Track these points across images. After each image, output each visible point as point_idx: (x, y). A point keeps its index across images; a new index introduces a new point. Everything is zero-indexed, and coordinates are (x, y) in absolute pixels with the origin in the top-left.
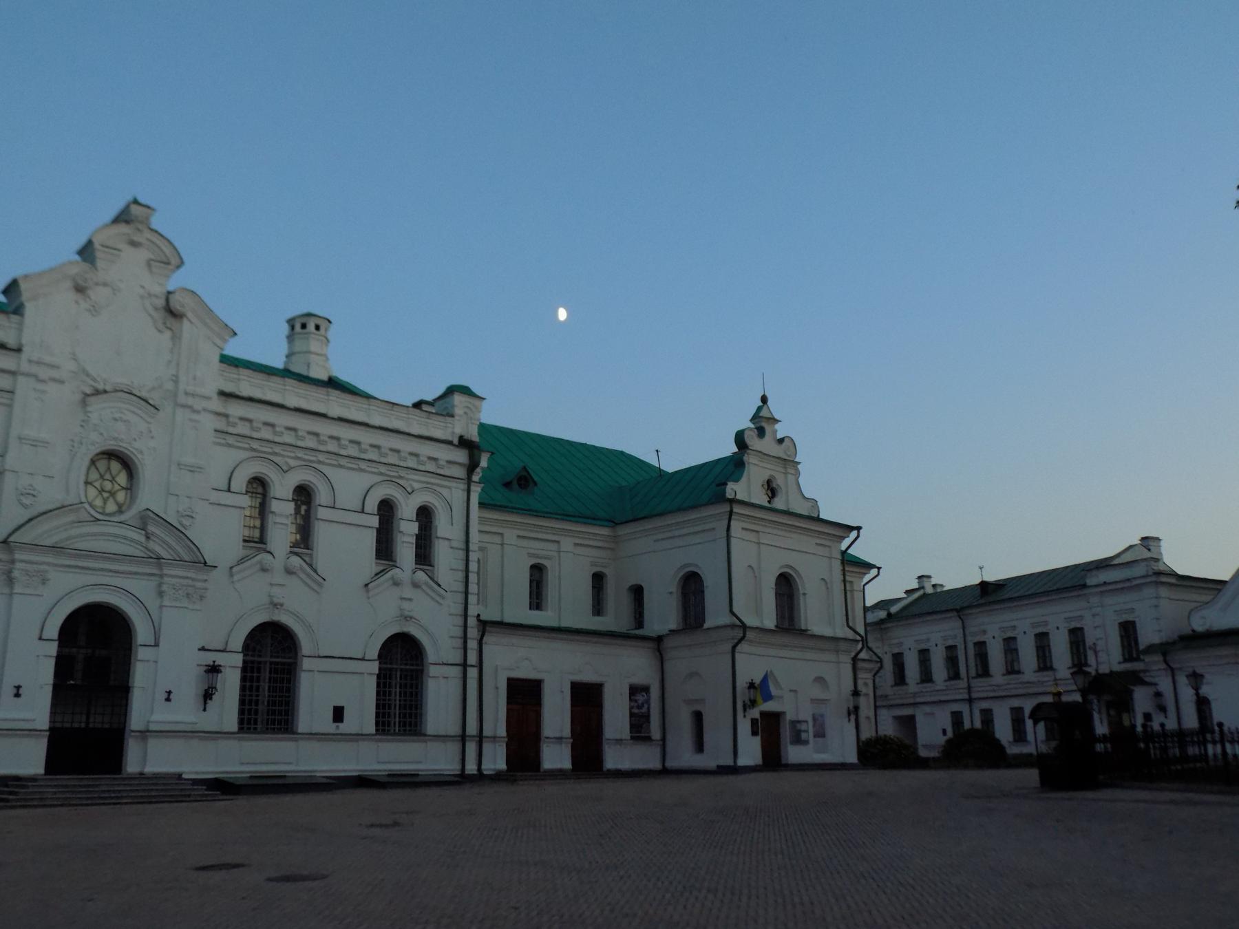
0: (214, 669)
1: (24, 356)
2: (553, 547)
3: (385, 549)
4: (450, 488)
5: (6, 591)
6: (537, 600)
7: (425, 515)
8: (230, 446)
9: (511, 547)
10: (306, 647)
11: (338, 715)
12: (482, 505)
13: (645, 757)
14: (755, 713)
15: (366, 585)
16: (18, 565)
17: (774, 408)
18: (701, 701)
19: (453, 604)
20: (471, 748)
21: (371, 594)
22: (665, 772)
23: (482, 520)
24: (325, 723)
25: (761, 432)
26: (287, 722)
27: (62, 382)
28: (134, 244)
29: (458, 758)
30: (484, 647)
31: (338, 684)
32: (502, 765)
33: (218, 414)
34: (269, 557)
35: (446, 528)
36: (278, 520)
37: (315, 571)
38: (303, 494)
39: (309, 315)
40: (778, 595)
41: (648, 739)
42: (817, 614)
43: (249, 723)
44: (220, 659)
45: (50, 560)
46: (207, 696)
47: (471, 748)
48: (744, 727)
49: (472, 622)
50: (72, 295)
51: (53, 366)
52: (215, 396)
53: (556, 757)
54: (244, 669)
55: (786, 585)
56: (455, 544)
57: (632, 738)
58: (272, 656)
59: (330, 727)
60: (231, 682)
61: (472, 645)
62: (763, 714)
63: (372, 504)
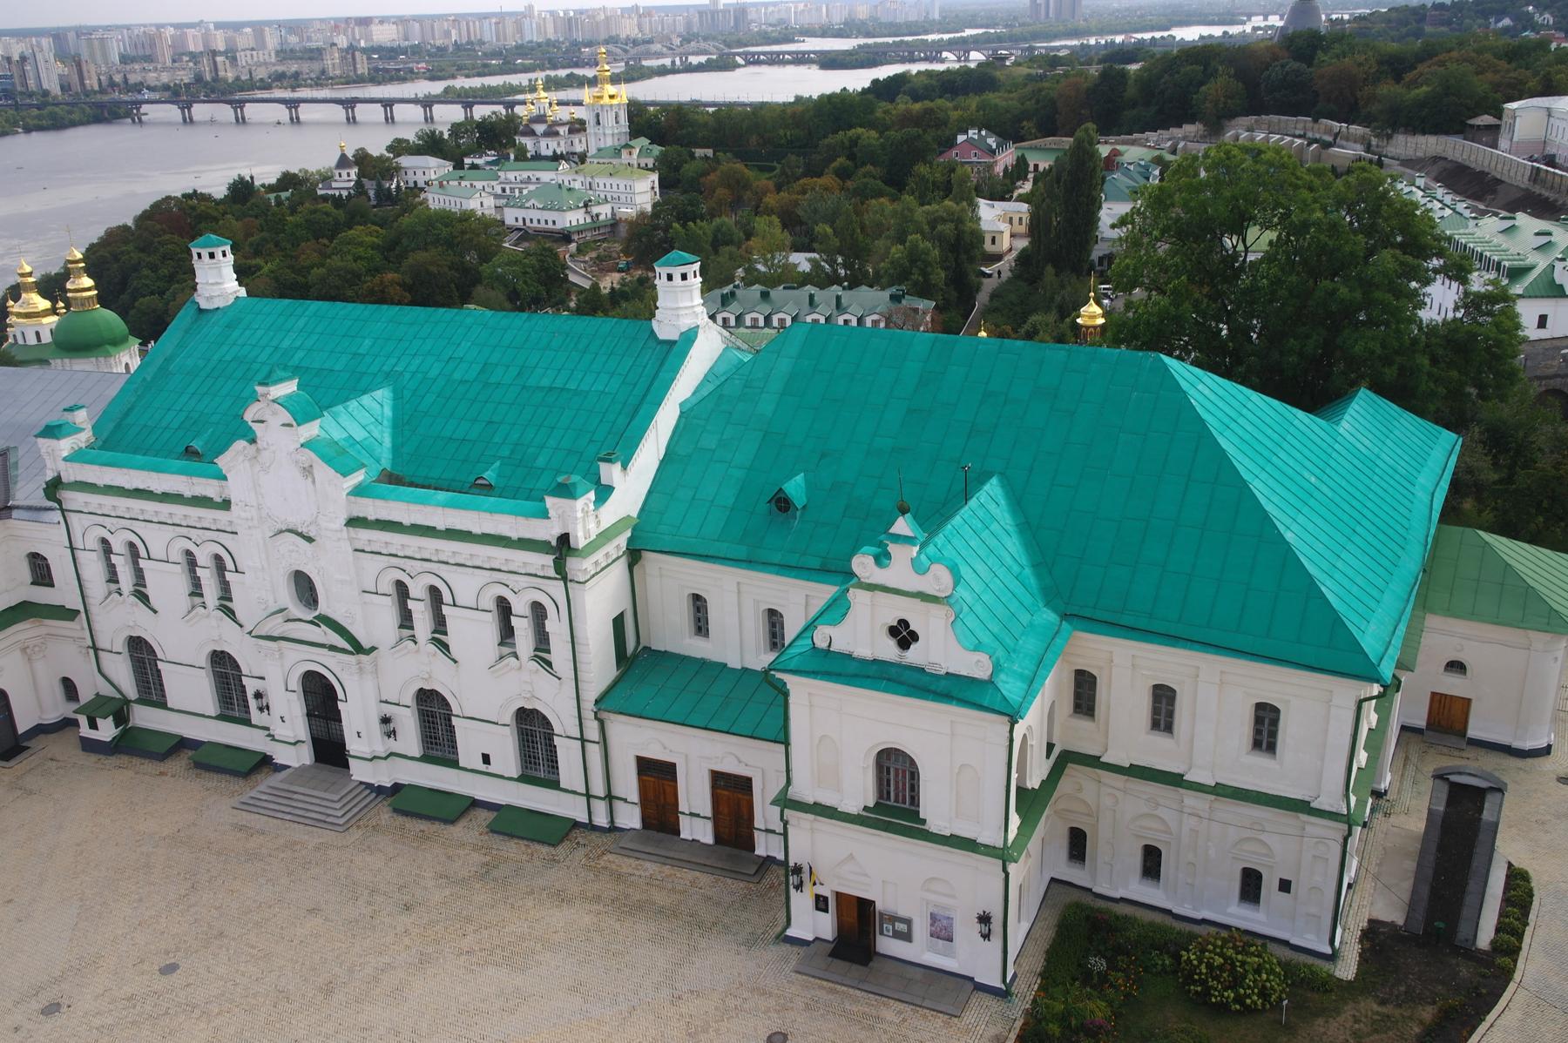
7: (538, 611)
10: (455, 710)
11: (486, 759)
35: (555, 626)
38: (435, 593)
44: (389, 710)
58: (434, 712)
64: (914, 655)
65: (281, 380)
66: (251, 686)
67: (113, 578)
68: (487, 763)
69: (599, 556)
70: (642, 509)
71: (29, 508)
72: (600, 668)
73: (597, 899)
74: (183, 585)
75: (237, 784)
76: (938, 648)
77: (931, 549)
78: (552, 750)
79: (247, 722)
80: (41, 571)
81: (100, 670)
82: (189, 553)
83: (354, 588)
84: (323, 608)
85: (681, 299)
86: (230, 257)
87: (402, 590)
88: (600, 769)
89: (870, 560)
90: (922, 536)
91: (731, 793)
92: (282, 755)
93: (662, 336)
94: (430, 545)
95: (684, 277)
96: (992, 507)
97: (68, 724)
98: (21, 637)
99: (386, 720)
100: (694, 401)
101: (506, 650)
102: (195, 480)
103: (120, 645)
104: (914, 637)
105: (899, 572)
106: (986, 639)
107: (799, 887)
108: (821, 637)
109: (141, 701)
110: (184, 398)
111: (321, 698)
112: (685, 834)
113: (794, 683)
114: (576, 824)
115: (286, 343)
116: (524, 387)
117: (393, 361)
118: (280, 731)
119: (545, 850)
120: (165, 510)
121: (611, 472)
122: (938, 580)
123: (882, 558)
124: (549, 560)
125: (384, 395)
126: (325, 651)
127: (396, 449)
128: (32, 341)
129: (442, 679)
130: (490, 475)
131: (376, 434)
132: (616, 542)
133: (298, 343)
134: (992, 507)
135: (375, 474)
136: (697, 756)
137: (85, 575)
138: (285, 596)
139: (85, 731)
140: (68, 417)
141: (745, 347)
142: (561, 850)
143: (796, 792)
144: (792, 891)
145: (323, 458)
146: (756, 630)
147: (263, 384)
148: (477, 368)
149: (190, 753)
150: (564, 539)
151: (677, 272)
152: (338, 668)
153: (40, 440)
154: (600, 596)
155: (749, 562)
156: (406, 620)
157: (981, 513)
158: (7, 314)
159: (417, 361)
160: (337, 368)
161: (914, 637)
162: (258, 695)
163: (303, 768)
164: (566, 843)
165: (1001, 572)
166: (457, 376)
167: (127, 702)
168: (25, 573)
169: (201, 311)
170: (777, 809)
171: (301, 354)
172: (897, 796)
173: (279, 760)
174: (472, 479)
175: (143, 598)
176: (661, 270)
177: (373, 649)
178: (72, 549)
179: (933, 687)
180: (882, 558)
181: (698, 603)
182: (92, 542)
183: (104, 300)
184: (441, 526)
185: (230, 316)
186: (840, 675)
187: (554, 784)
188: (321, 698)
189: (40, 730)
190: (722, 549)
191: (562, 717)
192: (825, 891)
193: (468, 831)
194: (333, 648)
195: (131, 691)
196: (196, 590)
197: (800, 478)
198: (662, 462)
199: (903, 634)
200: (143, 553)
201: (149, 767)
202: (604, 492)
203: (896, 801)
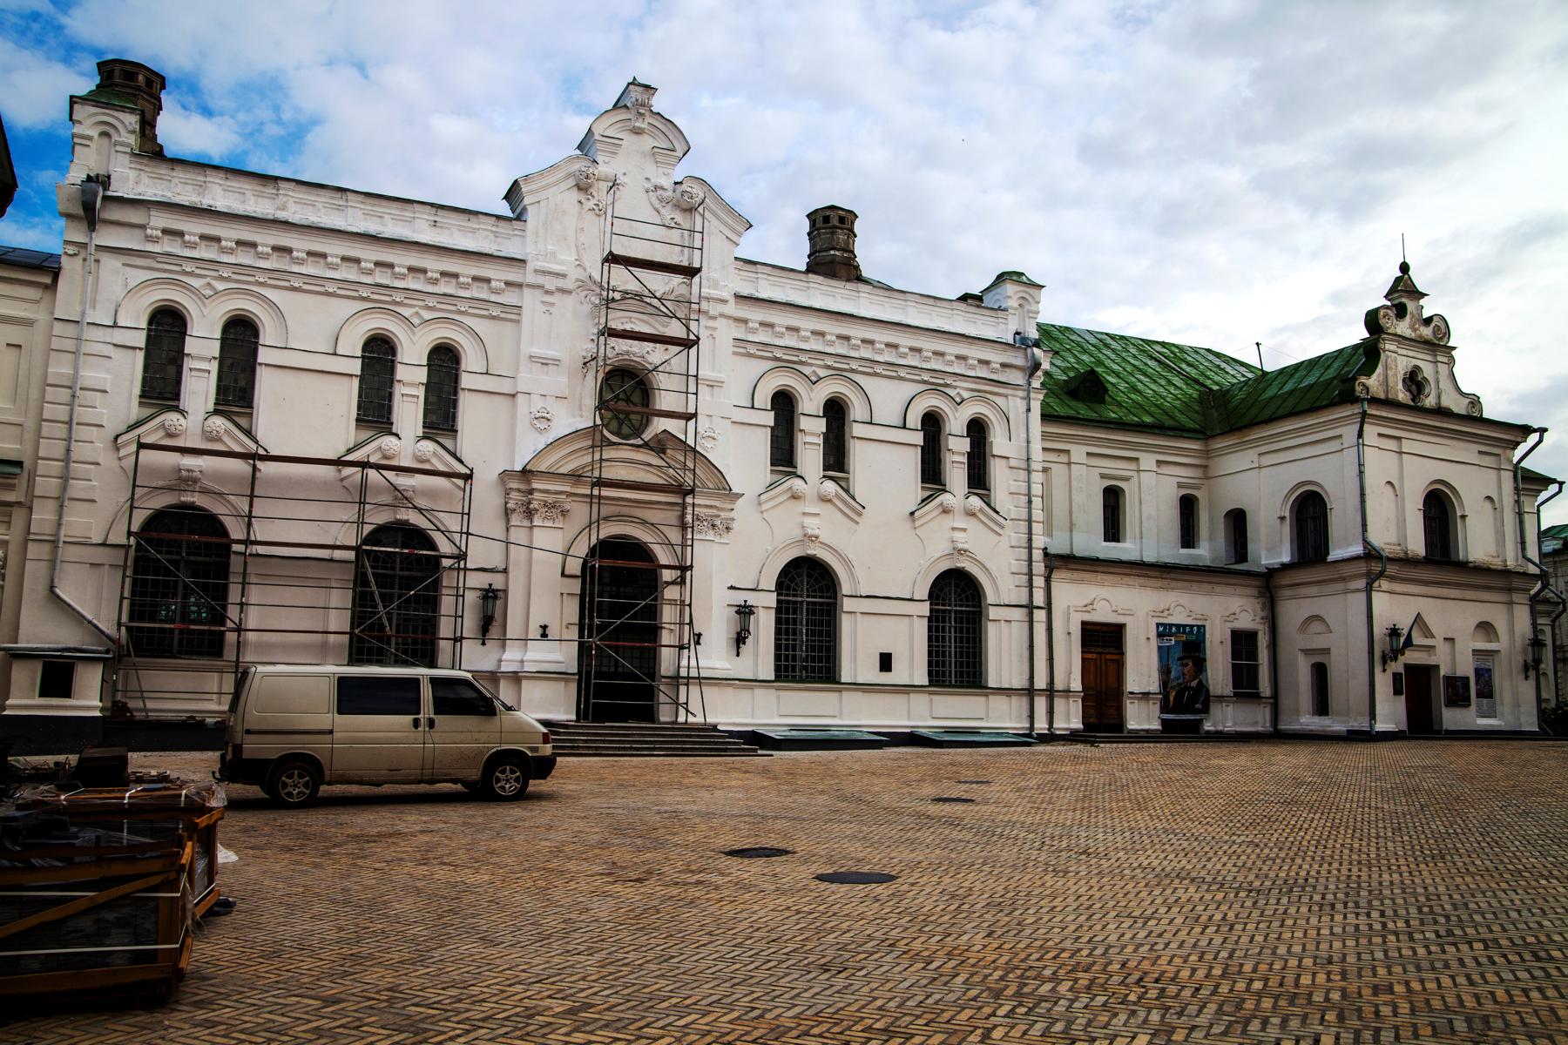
0: (745, 611)
1: (530, 266)
2: (1133, 466)
3: (932, 473)
4: (1006, 396)
5: (526, 523)
6: (1113, 530)
7: (977, 429)
8: (750, 355)
9: (1082, 470)
11: (886, 662)
12: (1046, 417)
13: (1254, 718)
14: (1397, 667)
15: (912, 514)
16: (537, 495)
17: (1419, 279)
18: (1327, 651)
19: (1014, 534)
20: (1041, 704)
21: (918, 523)
22: (1277, 736)
23: (1045, 436)
24: (873, 675)
25: (1401, 311)
26: (828, 671)
27: (569, 292)
28: (637, 132)
29: (1026, 713)
30: (1054, 585)
31: (882, 631)
32: (1077, 724)
33: (737, 320)
34: (799, 482)
36: (808, 439)
37: (853, 498)
38: (835, 411)
39: (832, 208)
40: (1428, 519)
41: (1255, 697)
42: (1480, 540)
43: (786, 670)
44: (752, 598)
45: (568, 489)
46: (740, 639)
47: (1041, 704)
48: (1383, 683)
49: (1037, 555)
50: (575, 195)
51: (557, 275)
52: (732, 300)
53: (1140, 717)
54: (778, 610)
55: (1439, 508)
56: (1013, 463)
57: (1236, 694)
58: (809, 592)
59: (873, 675)
60: (765, 626)
61: (1039, 582)
62: (1407, 667)
63: (914, 419)
67: (161, 388)
87: (784, 403)
112: (1132, 725)
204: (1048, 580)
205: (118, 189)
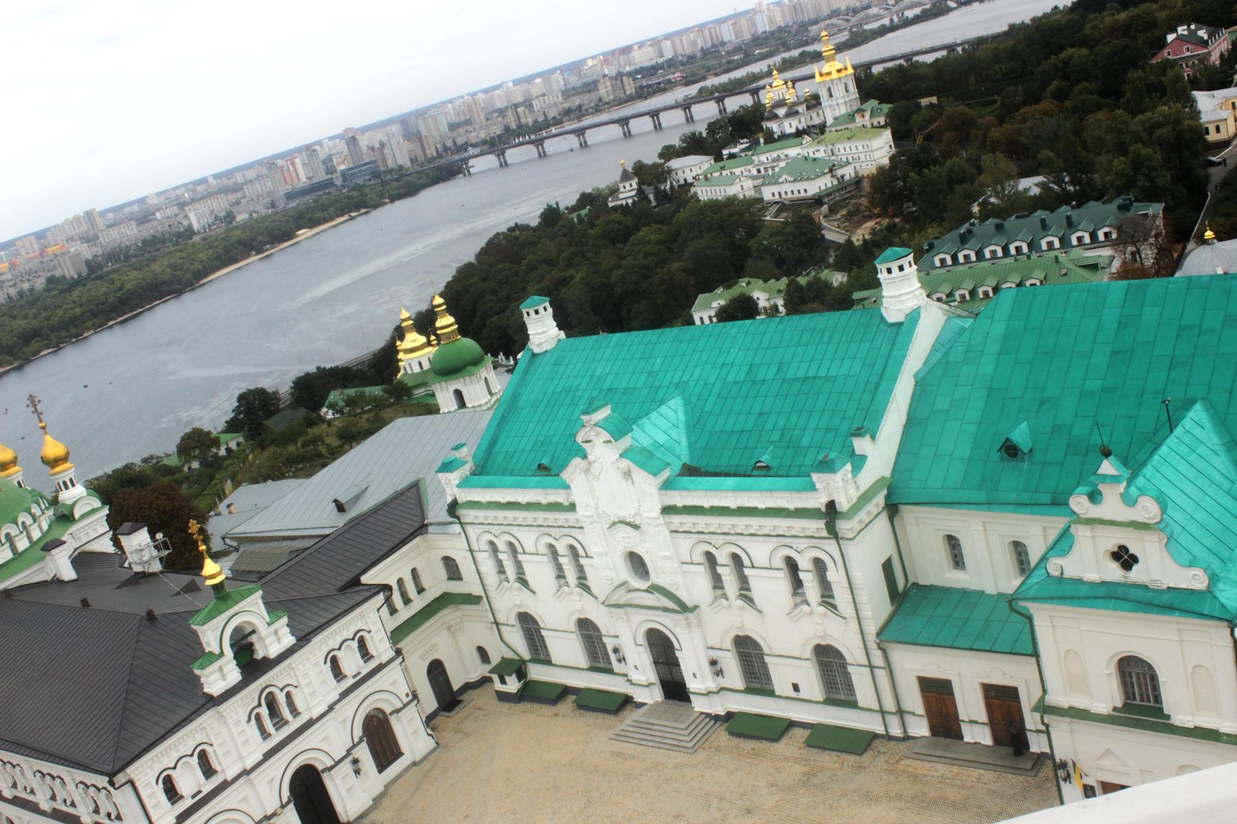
7: (819, 565)
10: (766, 650)
11: (796, 688)
38: (736, 558)
44: (715, 654)
58: (749, 652)
64: (1137, 574)
65: (599, 408)
66: (610, 643)
67: (502, 571)
68: (797, 692)
69: (863, 515)
70: (894, 469)
71: (439, 524)
72: (876, 606)
73: (899, 797)
74: (549, 571)
75: (610, 719)
76: (1158, 568)
77: (1140, 481)
78: (847, 675)
79: (609, 671)
80: (452, 569)
81: (502, 639)
82: (551, 546)
83: (674, 560)
84: (655, 578)
85: (901, 288)
86: (550, 310)
87: (711, 559)
88: (888, 689)
89: (1084, 500)
90: (1126, 473)
91: (1001, 701)
92: (640, 696)
93: (891, 320)
94: (728, 522)
95: (901, 268)
96: (1197, 431)
97: (485, 680)
98: (447, 619)
99: (713, 663)
100: (926, 369)
101: (799, 599)
102: (548, 491)
103: (513, 620)
104: (1134, 559)
105: (1111, 506)
106: (1200, 553)
107: (1068, 778)
108: (1054, 566)
109: (534, 660)
110: (532, 426)
111: (662, 650)
112: (967, 739)
113: (1035, 609)
114: (875, 736)
115: (598, 372)
116: (784, 380)
117: (680, 373)
118: (636, 677)
119: (852, 759)
120: (530, 516)
121: (862, 445)
122: (1147, 510)
123: (1094, 496)
124: (821, 524)
125: (676, 403)
126: (660, 613)
127: (691, 446)
128: (417, 369)
129: (753, 627)
130: (766, 459)
131: (675, 436)
132: (875, 501)
133: (607, 370)
134: (1197, 431)
135: (677, 469)
136: (969, 675)
137: (483, 568)
138: (624, 573)
139: (498, 686)
140: (457, 454)
141: (965, 313)
142: (866, 758)
143: (1051, 699)
144: (1062, 783)
145: (636, 463)
146: (1005, 561)
147: (586, 413)
148: (745, 369)
149: (574, 697)
150: (831, 505)
151: (894, 266)
152: (671, 625)
153: (440, 475)
154: (868, 547)
155: (989, 504)
156: (717, 582)
157: (1186, 439)
158: (397, 352)
159: (698, 371)
160: (639, 385)
161: (1134, 559)
162: (616, 650)
163: (656, 704)
164: (869, 752)
165: (1212, 490)
166: (730, 379)
167: (523, 662)
168: (442, 572)
169: (534, 355)
170: (1037, 715)
171: (610, 378)
172: (1141, 696)
173: (638, 699)
174: (752, 463)
175: (523, 581)
176: (881, 267)
177: (696, 607)
178: (471, 551)
179: (1156, 602)
180: (1094, 496)
181: (953, 542)
182: (484, 546)
183: (463, 331)
184: (733, 505)
185: (557, 356)
186: (1073, 598)
187: (853, 704)
188: (662, 650)
189: (468, 687)
190: (965, 495)
191: (851, 649)
192: (1090, 781)
193: (791, 746)
194: (665, 610)
195: (526, 655)
196: (561, 576)
197: (1024, 426)
198: (905, 427)
199: (1125, 558)
200: (519, 549)
201: (546, 710)
202: (858, 461)
203: (1142, 700)
204: (884, 651)
205: (459, 501)
